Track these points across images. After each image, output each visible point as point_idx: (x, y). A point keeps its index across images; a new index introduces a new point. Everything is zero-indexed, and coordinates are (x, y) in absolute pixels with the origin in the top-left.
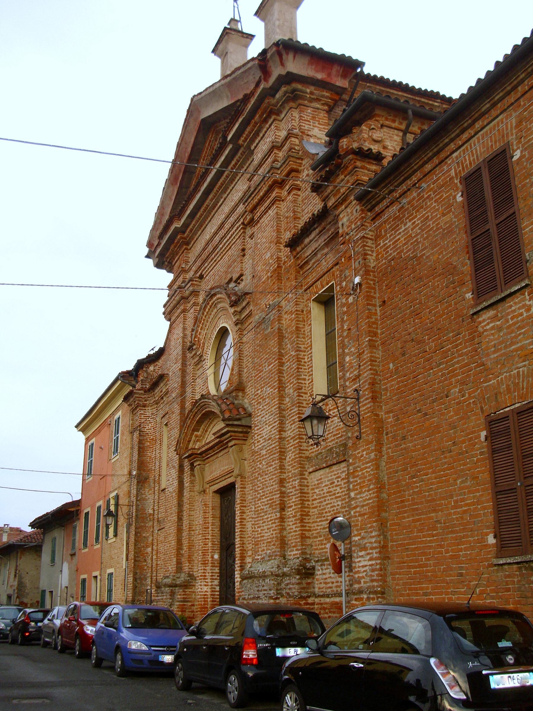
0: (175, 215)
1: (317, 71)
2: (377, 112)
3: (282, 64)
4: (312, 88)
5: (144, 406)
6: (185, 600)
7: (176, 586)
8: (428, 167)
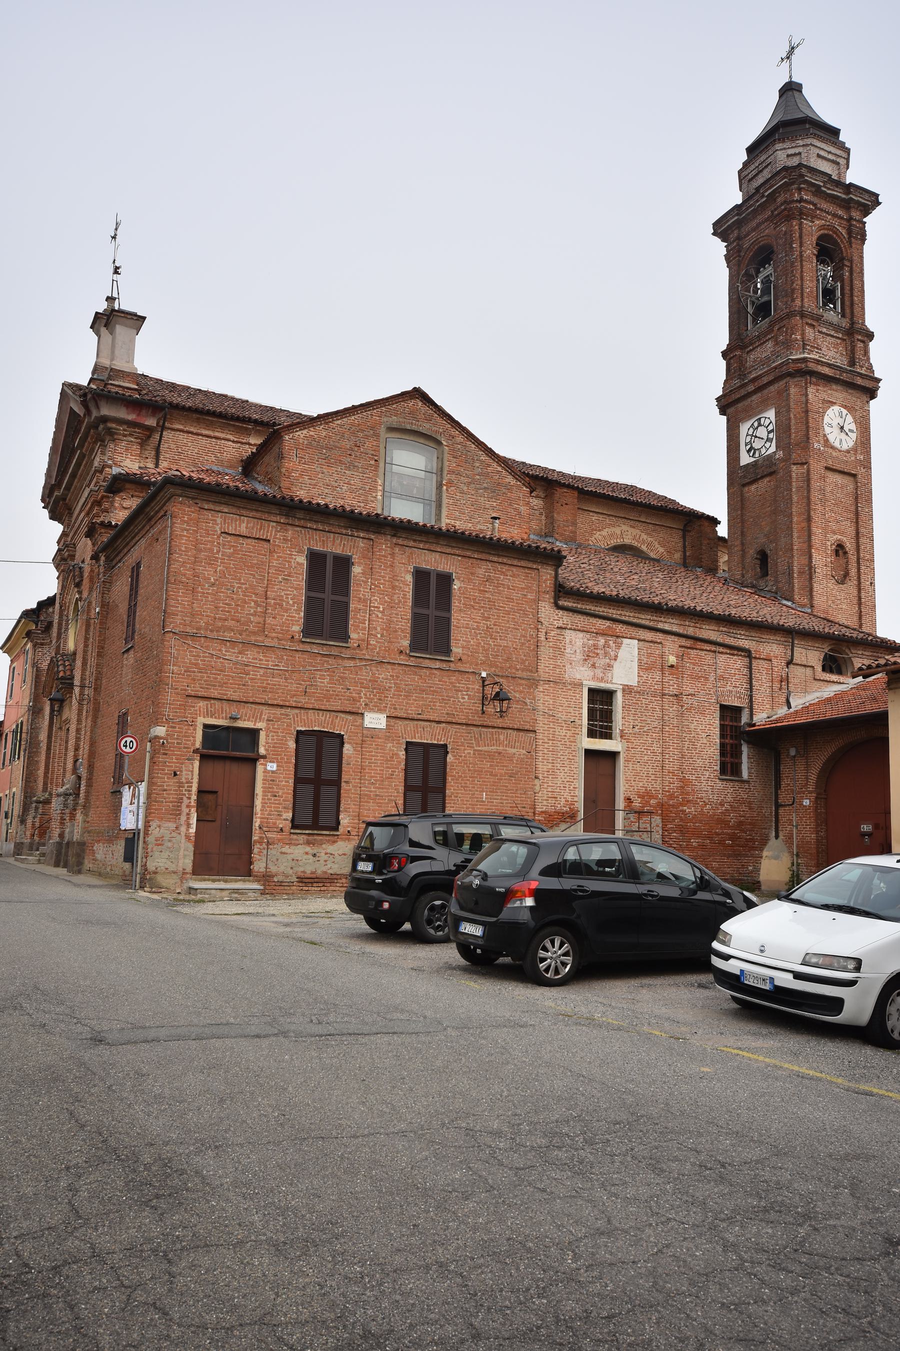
0: (58, 485)
1: (128, 414)
2: (128, 486)
3: (98, 408)
4: (125, 427)
5: (42, 644)
6: (43, 814)
7: (40, 802)
8: (126, 550)
